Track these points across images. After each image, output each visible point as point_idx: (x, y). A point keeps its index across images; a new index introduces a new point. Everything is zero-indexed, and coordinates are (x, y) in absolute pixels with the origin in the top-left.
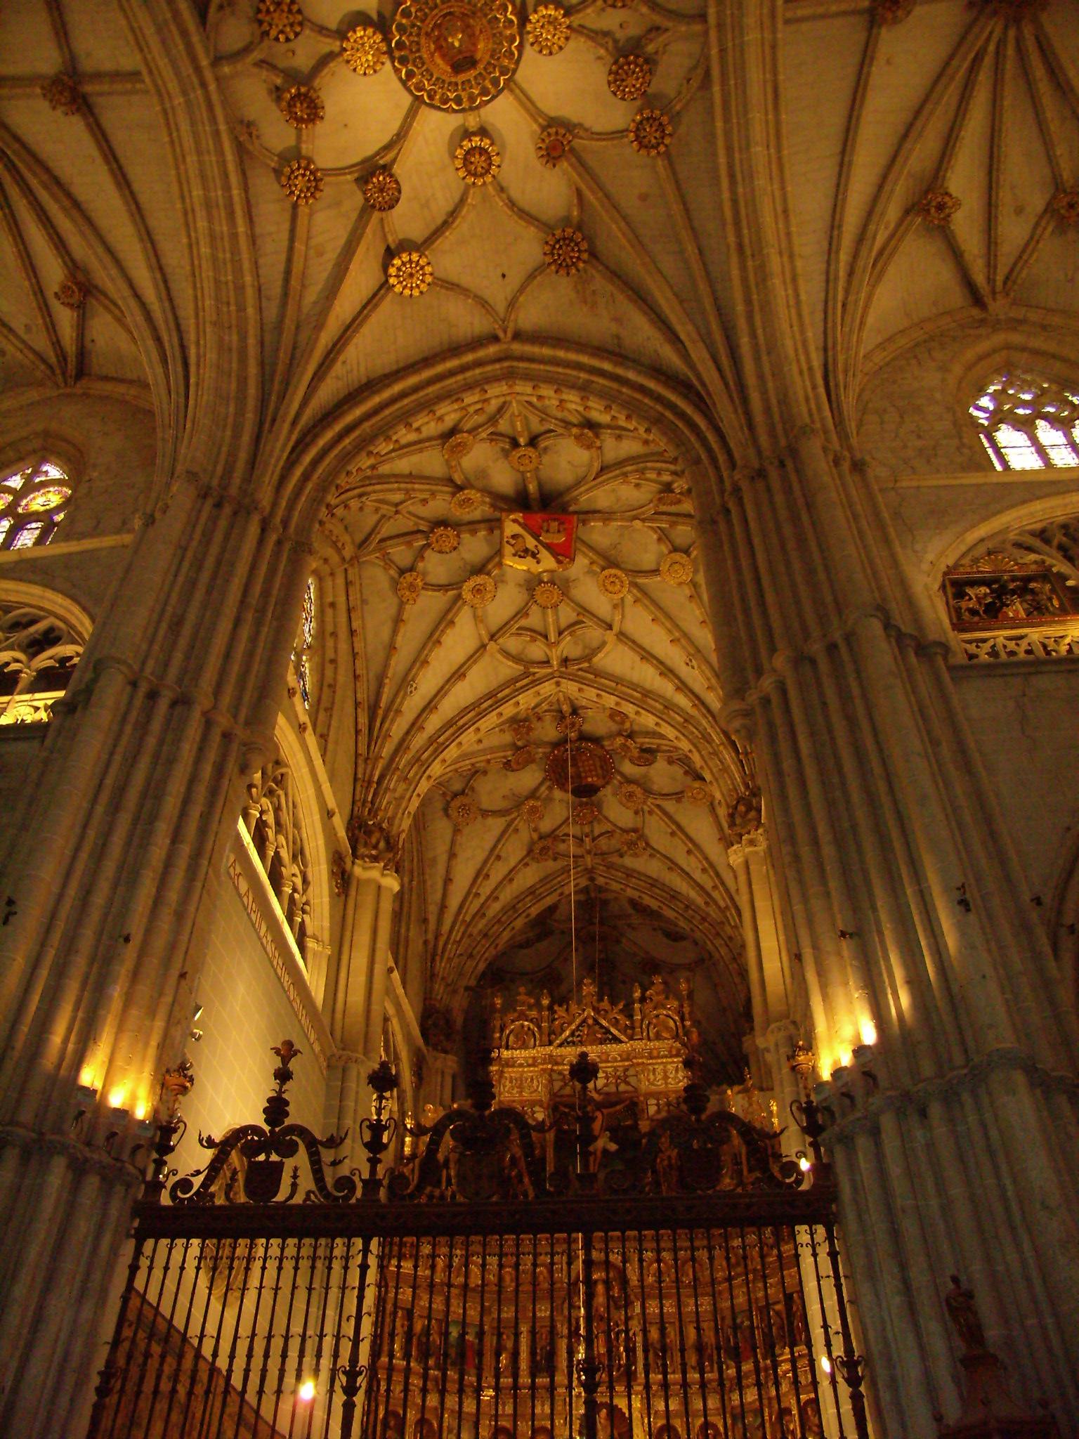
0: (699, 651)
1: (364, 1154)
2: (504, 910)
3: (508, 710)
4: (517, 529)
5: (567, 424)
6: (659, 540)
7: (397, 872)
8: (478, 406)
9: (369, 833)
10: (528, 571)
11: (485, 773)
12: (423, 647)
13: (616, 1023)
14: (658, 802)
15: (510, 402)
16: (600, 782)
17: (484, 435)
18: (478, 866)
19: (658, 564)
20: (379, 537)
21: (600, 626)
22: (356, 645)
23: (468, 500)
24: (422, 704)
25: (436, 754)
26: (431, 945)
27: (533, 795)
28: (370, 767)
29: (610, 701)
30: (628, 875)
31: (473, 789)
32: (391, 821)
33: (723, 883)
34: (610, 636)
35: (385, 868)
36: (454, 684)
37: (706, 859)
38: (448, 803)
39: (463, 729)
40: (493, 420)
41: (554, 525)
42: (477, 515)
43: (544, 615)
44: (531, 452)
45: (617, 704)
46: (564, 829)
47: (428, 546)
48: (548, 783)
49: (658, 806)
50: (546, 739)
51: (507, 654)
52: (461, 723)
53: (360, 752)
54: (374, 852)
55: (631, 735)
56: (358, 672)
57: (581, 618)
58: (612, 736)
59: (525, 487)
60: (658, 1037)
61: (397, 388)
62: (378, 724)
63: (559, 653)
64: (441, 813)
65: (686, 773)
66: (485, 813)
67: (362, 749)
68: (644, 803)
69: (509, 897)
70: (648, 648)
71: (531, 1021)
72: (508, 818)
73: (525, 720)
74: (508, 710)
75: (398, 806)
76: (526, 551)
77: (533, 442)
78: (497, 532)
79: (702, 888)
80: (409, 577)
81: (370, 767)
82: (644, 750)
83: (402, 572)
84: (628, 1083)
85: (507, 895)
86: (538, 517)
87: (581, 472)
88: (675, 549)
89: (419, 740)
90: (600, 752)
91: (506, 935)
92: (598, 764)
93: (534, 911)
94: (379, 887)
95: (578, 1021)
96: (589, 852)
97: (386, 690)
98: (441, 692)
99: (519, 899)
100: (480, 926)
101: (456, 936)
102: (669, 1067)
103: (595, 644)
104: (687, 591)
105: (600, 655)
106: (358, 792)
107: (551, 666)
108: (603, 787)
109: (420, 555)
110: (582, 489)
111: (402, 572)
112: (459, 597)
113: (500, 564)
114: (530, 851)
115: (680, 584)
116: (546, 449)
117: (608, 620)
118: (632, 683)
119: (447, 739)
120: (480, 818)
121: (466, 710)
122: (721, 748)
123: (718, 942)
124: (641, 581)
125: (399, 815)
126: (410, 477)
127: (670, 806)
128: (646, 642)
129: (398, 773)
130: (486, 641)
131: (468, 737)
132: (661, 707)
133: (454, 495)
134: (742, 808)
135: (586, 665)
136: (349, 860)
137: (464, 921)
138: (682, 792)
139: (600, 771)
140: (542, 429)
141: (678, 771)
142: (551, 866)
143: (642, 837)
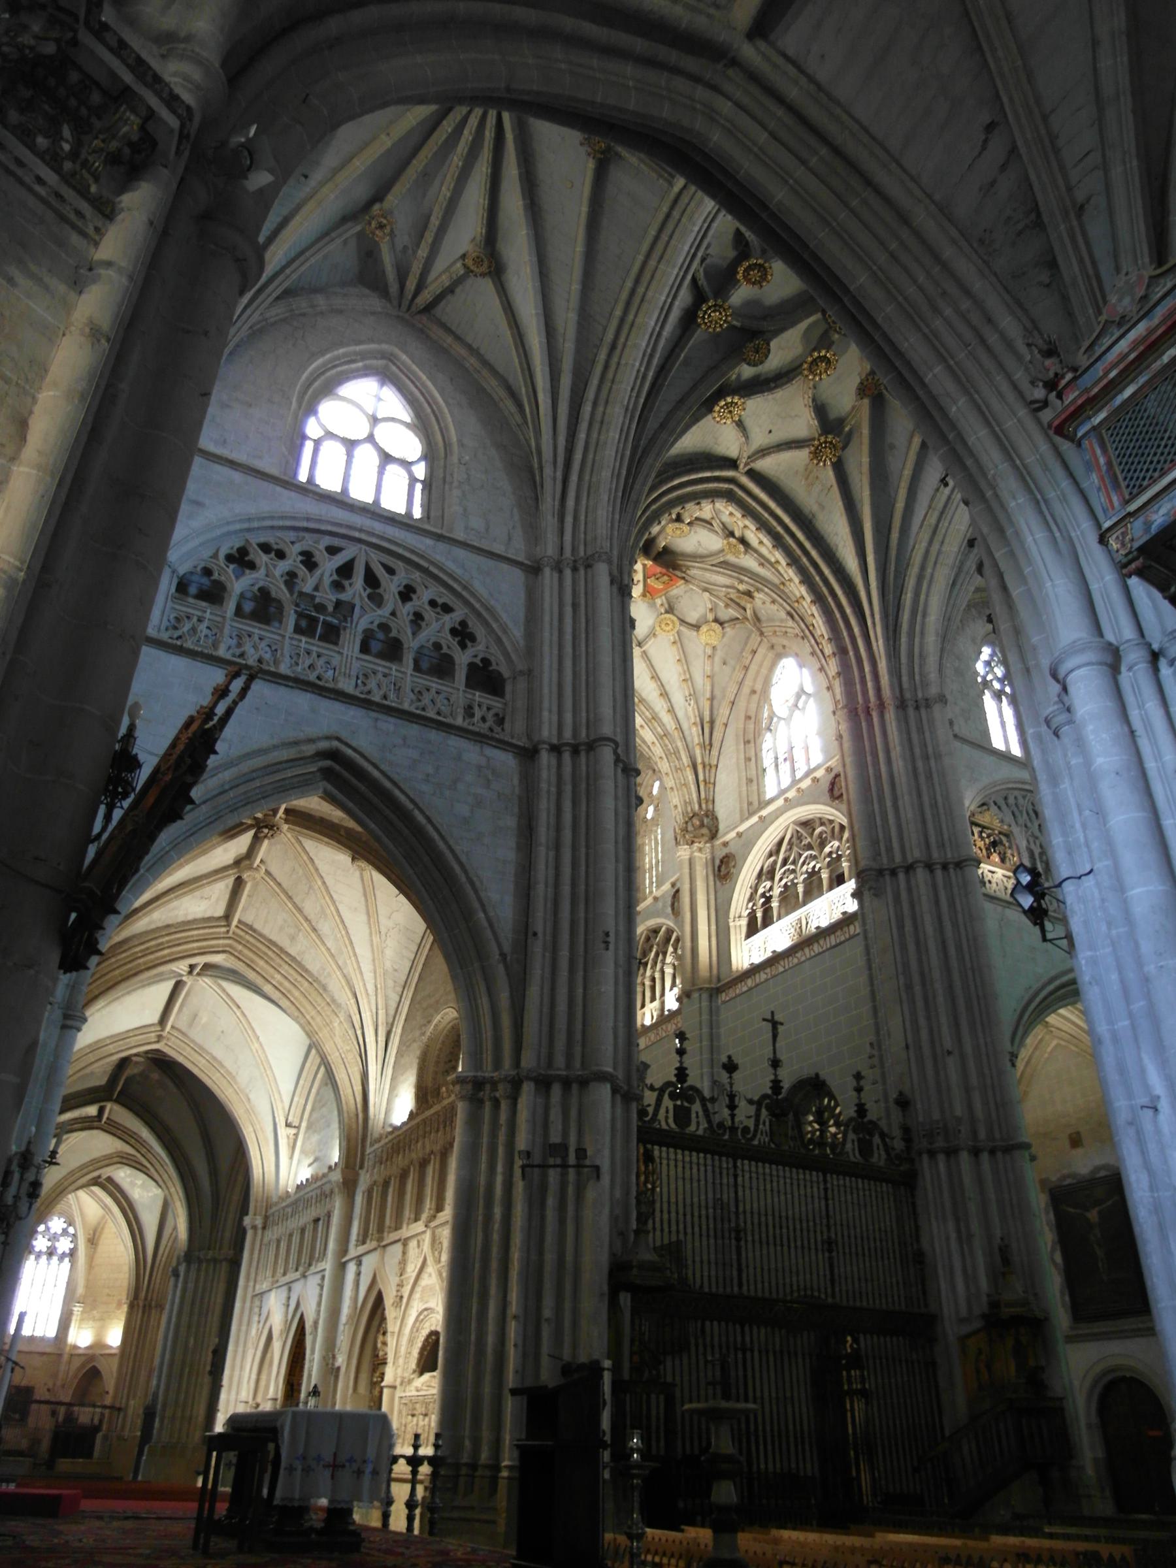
1: (726, 1112)
6: (711, 610)
87: (701, 551)
88: (716, 620)
124: (683, 629)
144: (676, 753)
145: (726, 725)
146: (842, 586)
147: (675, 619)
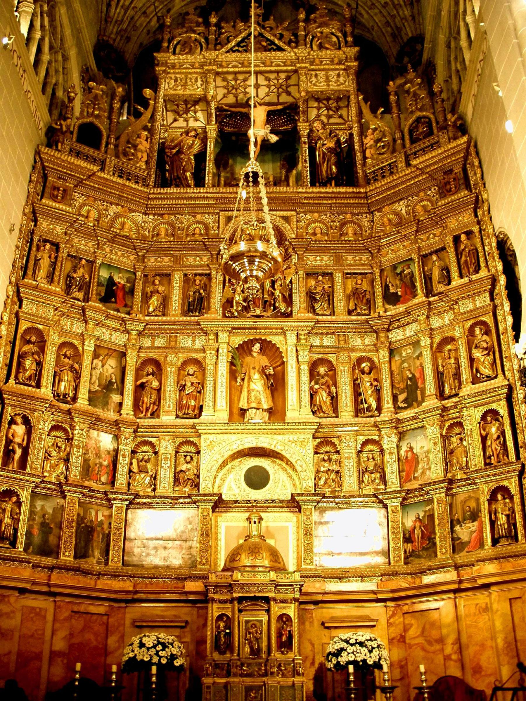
13: (281, 38)
60: (321, 47)
71: (199, 34)
84: (289, 94)
95: (243, 35)
102: (331, 73)
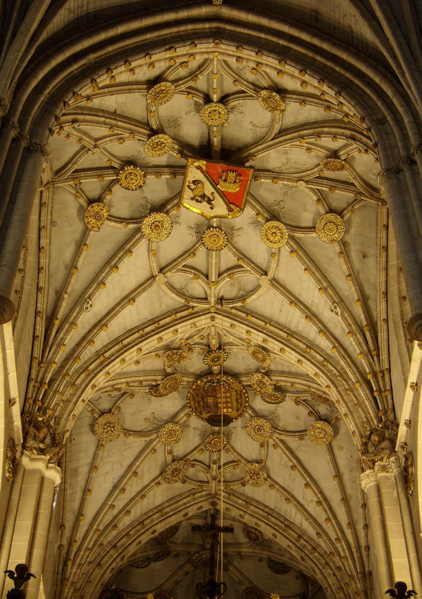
0: (342, 301)
2: (132, 526)
3: (168, 336)
4: (199, 176)
5: (257, 88)
7: (59, 465)
8: (185, 59)
9: (38, 428)
10: (202, 215)
11: (132, 395)
12: (101, 270)
14: (281, 437)
15: (212, 61)
16: (234, 414)
17: (183, 88)
18: (116, 481)
19: (315, 222)
20: (75, 167)
21: (257, 271)
22: (41, 261)
23: (160, 144)
24: (94, 321)
25: (103, 365)
26: (64, 551)
27: (172, 419)
28: (43, 370)
29: (258, 338)
30: (247, 503)
31: (119, 408)
32: (58, 420)
33: (335, 517)
34: (264, 281)
35: (49, 461)
36: (123, 308)
37: (321, 493)
38: (95, 419)
39: (127, 348)
40: (193, 75)
41: (232, 175)
42: (163, 160)
43: (208, 256)
44: (220, 108)
45: (264, 341)
46: (197, 455)
47: (117, 181)
48: (187, 410)
49: (282, 441)
50: (191, 370)
51: (171, 287)
52: (125, 342)
53: (35, 355)
54: (42, 446)
55: (268, 373)
56: (41, 285)
57: (241, 263)
58: (248, 373)
59: (209, 140)
61: (121, 29)
62: (53, 333)
63: (217, 292)
64: (87, 429)
65: (310, 413)
66: (128, 432)
67: (37, 353)
68: (271, 437)
69: (138, 513)
70: (297, 295)
72: (148, 439)
73: (178, 349)
74: (168, 336)
75: (64, 409)
76: (203, 196)
77: (224, 99)
78: (180, 178)
79: (315, 520)
80: (96, 207)
81: (43, 370)
82: (278, 388)
83: (91, 202)
85: (137, 511)
86: (220, 167)
87: (261, 132)
88: (331, 211)
89: (88, 352)
90: (237, 386)
91: (133, 549)
92: (234, 397)
93: (160, 528)
94: (43, 479)
96: (214, 478)
97: (64, 304)
98: (112, 313)
99: (148, 515)
100: (110, 538)
101: (89, 543)
103: (249, 287)
104: (338, 248)
105: (254, 297)
106: (30, 391)
107: (209, 303)
108: (236, 418)
109: (108, 188)
110: (260, 147)
111: (91, 202)
112: (138, 230)
113: (179, 205)
114: (162, 472)
115: (333, 241)
116: (233, 108)
117: (264, 267)
118: (279, 324)
119: (112, 355)
120: (122, 435)
121: (130, 332)
122: (357, 385)
123: (328, 571)
124: (297, 235)
125: (65, 416)
126: (114, 115)
127: (292, 442)
128: (295, 289)
129: (68, 378)
130: (156, 272)
131: (131, 355)
132: (304, 347)
133: (149, 137)
134: (375, 438)
135: (239, 304)
136: (19, 448)
137: (97, 530)
138: (306, 430)
139: (235, 404)
140: (235, 89)
141: (303, 411)
142: (178, 487)
143: (265, 468)
144: (343, 375)
145: (387, 321)
146: (364, 61)
147: (281, 226)
